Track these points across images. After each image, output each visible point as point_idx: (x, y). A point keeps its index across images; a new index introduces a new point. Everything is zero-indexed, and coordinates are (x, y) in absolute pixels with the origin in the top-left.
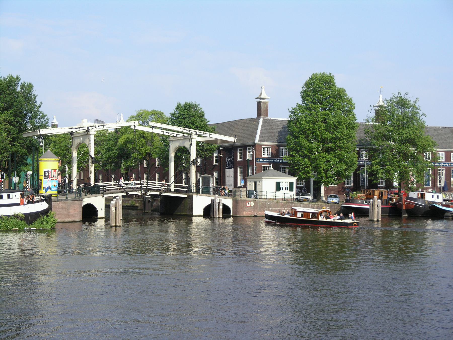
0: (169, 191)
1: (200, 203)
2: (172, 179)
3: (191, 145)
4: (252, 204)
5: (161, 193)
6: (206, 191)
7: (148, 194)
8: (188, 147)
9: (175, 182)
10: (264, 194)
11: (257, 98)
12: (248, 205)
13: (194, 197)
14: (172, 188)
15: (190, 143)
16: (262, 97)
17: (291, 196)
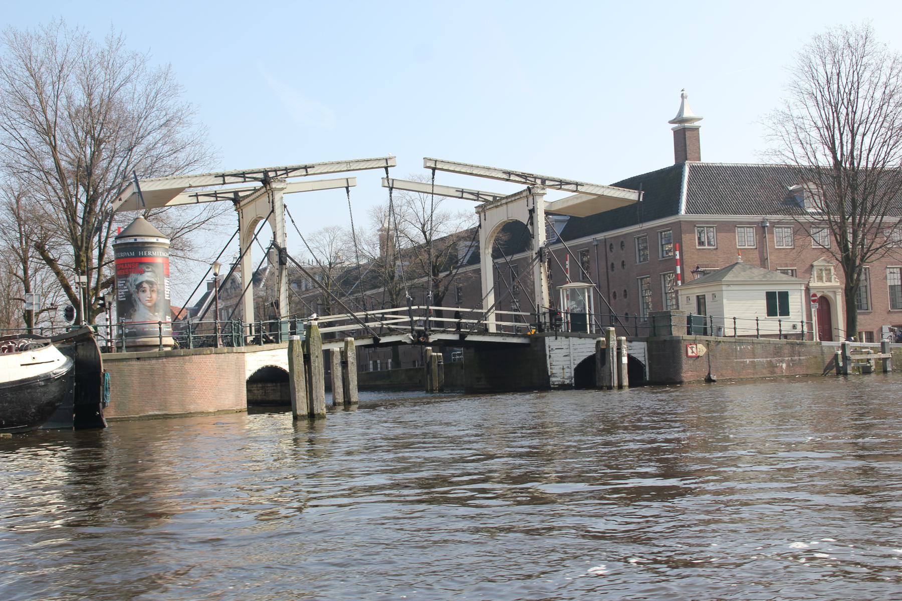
0: (485, 331)
1: (564, 354)
2: (491, 300)
3: (532, 211)
4: (701, 349)
5: (463, 336)
6: (578, 324)
7: (431, 340)
8: (524, 219)
9: (498, 305)
10: (728, 325)
11: (671, 122)
12: (690, 354)
13: (549, 341)
14: (492, 323)
15: (531, 207)
16: (686, 114)
17: (794, 327)
